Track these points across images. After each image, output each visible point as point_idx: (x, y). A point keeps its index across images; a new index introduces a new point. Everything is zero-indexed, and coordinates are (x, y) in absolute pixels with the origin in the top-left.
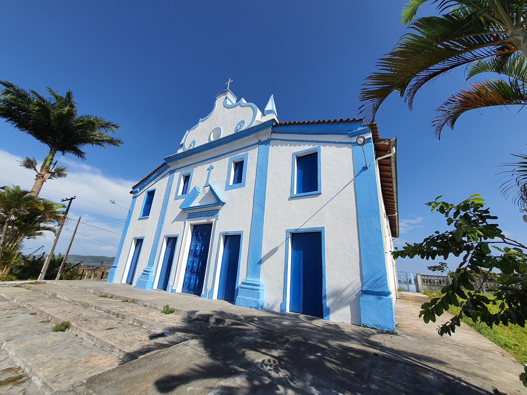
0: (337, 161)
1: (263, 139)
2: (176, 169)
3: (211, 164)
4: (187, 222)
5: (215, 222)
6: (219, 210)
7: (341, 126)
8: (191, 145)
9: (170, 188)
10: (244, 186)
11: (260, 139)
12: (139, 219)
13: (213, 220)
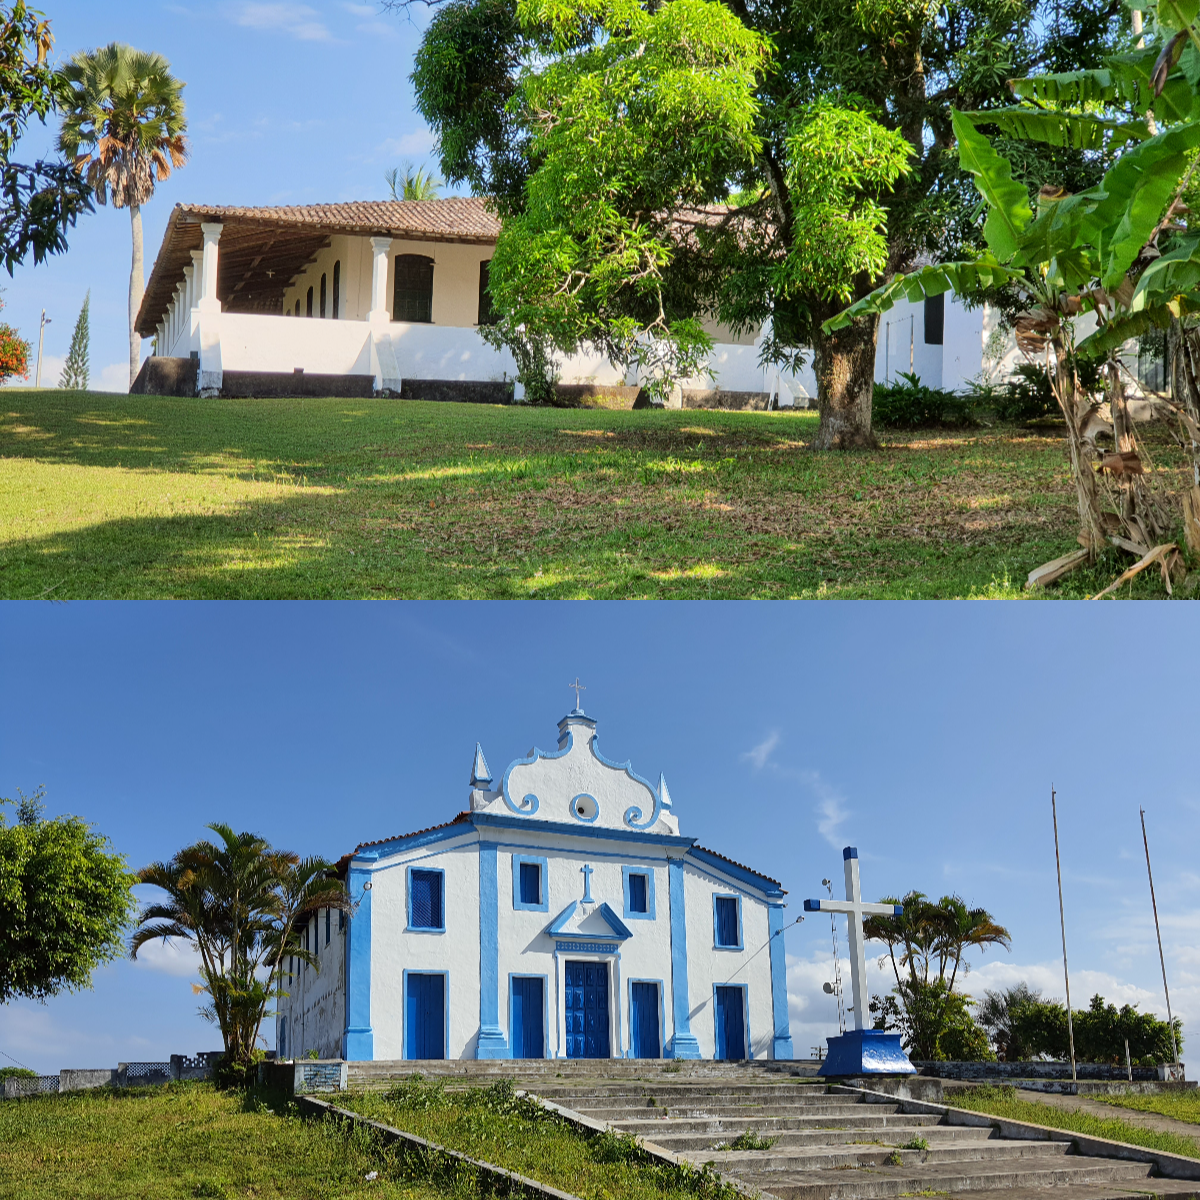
0: (753, 915)
1: (676, 856)
2: (501, 844)
3: (587, 863)
4: (559, 956)
5: (616, 962)
6: (617, 947)
7: (762, 882)
8: (525, 802)
9: (493, 881)
10: (654, 919)
11: (671, 855)
12: (407, 931)
13: (611, 959)
